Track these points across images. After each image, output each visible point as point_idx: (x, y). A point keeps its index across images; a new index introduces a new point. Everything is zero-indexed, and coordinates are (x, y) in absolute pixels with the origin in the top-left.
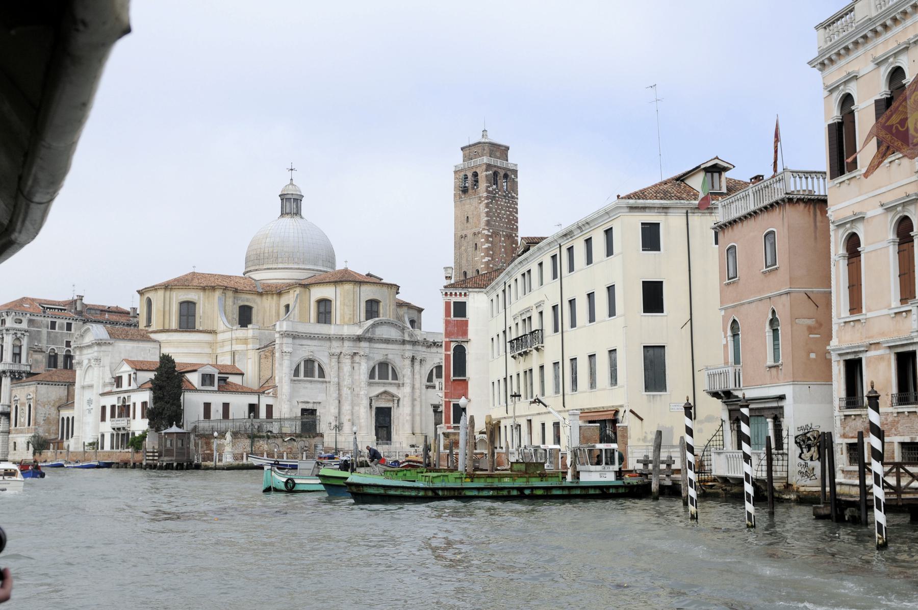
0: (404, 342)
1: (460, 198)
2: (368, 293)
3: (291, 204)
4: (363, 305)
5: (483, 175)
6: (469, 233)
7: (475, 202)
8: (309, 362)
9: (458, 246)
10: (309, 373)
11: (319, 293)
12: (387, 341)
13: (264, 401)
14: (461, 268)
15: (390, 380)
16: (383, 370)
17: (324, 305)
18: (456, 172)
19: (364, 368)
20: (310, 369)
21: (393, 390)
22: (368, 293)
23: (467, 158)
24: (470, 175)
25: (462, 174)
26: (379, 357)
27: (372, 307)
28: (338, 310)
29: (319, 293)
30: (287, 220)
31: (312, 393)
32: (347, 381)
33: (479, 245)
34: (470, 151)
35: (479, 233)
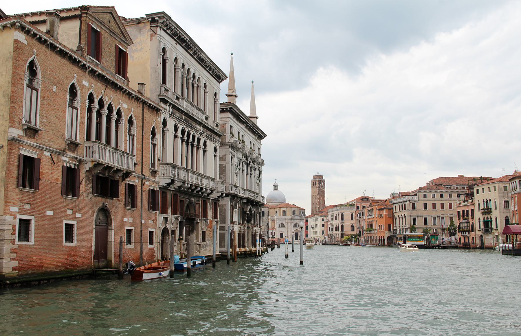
2: (293, 209)
3: (276, 187)
5: (317, 183)
8: (282, 224)
9: (312, 197)
10: (282, 226)
11: (283, 209)
13: (274, 231)
17: (284, 212)
19: (293, 225)
20: (282, 225)
22: (293, 209)
23: (314, 178)
27: (294, 212)
28: (287, 212)
29: (283, 209)
30: (275, 191)
31: (282, 230)
34: (315, 177)
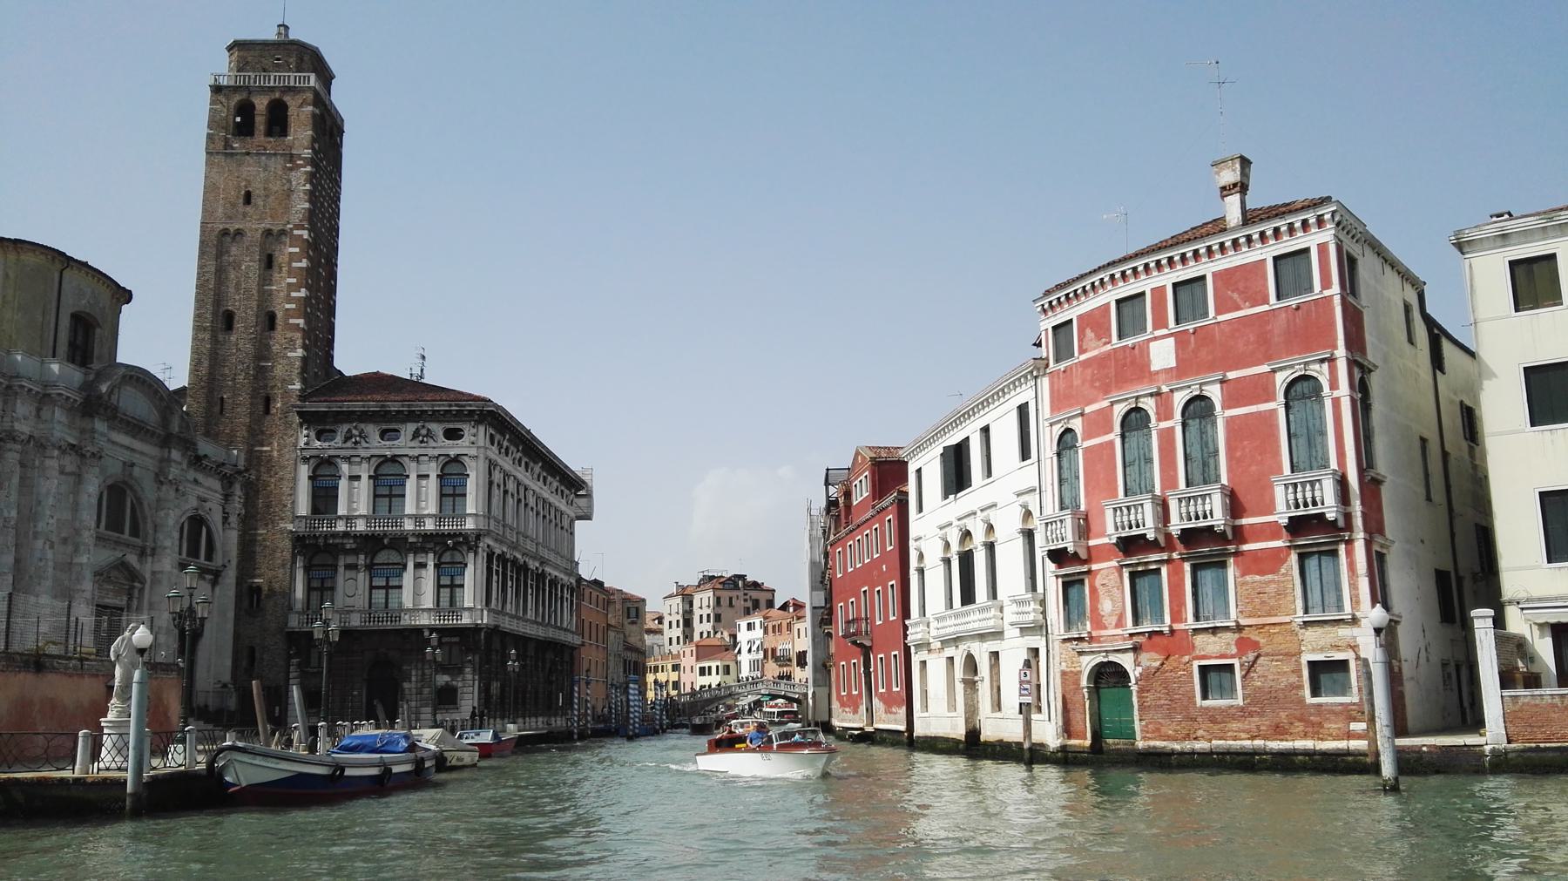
0: (166, 441)
1: (227, 145)
4: (65, 322)
6: (254, 227)
7: (276, 165)
12: (136, 428)
14: (218, 300)
15: (126, 536)
16: (121, 509)
18: (217, 89)
19: (92, 487)
21: (132, 559)
24: (261, 103)
25: (237, 98)
26: (115, 469)
32: (50, 520)
33: (281, 258)
35: (283, 232)
